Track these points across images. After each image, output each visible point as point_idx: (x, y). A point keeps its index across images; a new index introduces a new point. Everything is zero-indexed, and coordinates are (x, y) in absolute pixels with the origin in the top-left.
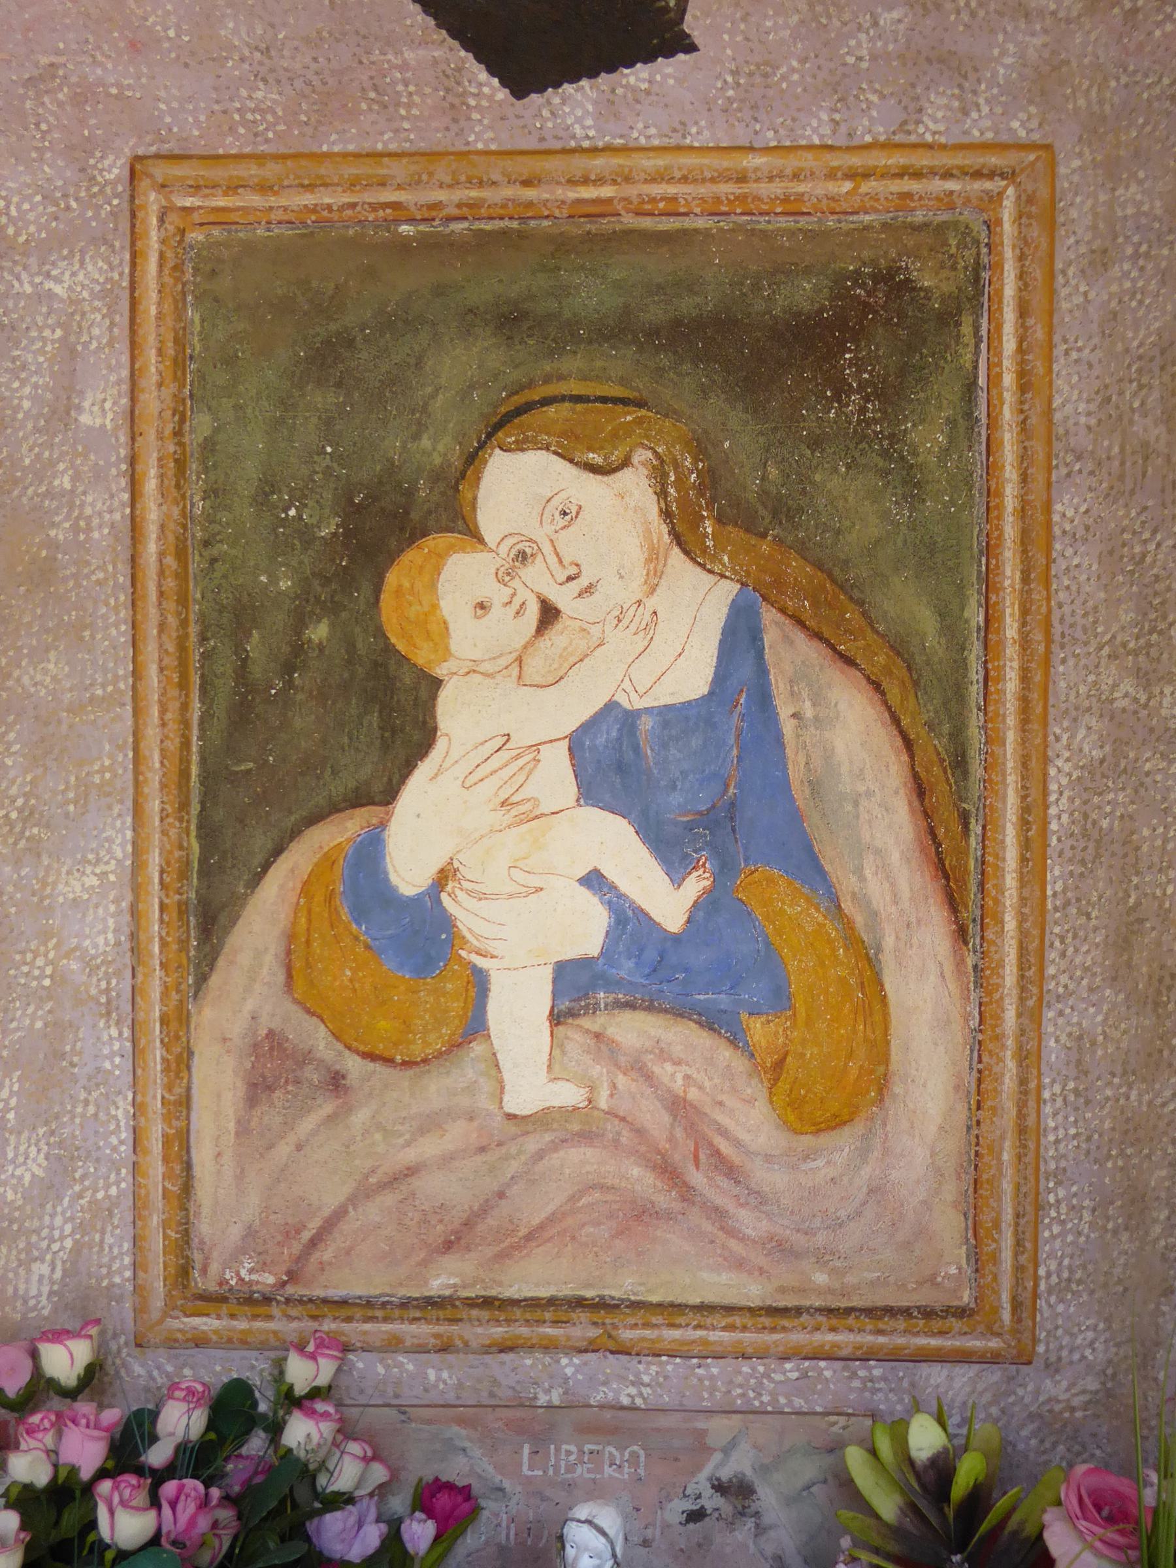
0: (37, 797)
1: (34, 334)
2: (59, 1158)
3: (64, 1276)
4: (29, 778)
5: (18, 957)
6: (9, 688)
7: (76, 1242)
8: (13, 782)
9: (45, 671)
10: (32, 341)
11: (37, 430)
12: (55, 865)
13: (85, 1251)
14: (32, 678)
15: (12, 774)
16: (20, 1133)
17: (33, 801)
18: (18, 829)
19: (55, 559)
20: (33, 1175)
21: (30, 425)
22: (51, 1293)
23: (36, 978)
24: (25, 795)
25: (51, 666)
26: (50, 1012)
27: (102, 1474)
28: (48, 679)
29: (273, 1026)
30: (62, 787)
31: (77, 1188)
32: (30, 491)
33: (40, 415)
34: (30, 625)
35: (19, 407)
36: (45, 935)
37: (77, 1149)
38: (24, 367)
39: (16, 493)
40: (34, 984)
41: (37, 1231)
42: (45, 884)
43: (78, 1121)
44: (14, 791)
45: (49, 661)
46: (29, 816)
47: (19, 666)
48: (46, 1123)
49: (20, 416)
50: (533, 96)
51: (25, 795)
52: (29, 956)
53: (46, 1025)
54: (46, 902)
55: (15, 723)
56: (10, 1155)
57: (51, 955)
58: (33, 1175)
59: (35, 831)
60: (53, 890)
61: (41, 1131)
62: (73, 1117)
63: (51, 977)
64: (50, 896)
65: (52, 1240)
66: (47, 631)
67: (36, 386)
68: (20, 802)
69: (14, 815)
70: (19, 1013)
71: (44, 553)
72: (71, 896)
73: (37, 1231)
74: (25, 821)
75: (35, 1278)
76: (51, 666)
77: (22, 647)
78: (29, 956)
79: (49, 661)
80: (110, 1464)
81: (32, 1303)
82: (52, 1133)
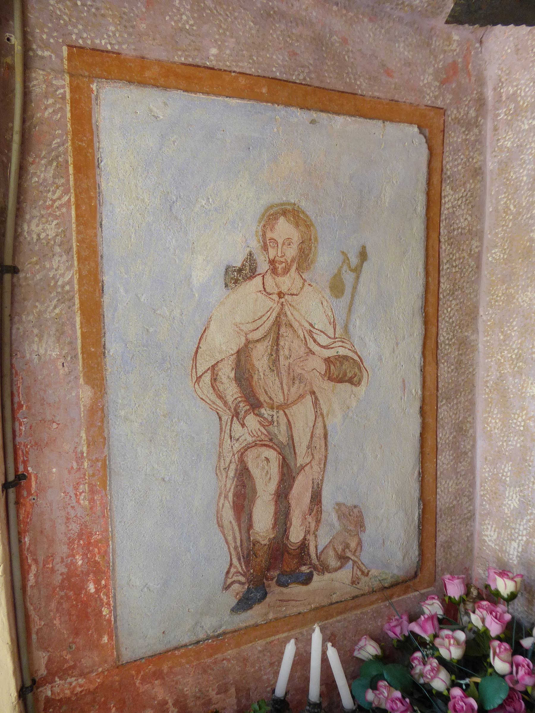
0: (522, 350)
1: (528, 146)
2: (523, 502)
3: (522, 552)
4: (519, 342)
5: (513, 416)
6: (514, 303)
7: (527, 539)
8: (514, 342)
9: (527, 296)
10: (528, 150)
11: (529, 189)
12: (527, 380)
13: (530, 544)
14: (522, 299)
15: (514, 339)
16: (510, 487)
17: (520, 352)
18: (515, 363)
19: (532, 246)
20: (514, 505)
21: (526, 188)
22: (517, 556)
23: (518, 426)
24: (518, 348)
25: (529, 293)
26: (522, 441)
27: (498, 638)
28: (528, 299)
29: (340, 499)
30: (531, 346)
31: (529, 517)
32: (524, 217)
33: (529, 182)
34: (522, 275)
35: (522, 180)
36: (522, 409)
37: (530, 501)
38: (524, 162)
39: (520, 219)
40: (517, 428)
41: (514, 529)
42: (523, 387)
43: (530, 489)
44: (514, 346)
45: (528, 291)
46: (519, 357)
47: (518, 294)
48: (519, 487)
49: (523, 184)
50: (524, 26)
51: (518, 348)
52: (516, 416)
53: (521, 446)
54: (523, 395)
55: (516, 317)
56: (507, 495)
57: (524, 417)
58: (514, 505)
59: (521, 364)
60: (526, 390)
61: (518, 489)
62: (529, 487)
63: (523, 426)
64: (524, 392)
65: (519, 535)
66: (528, 278)
67: (528, 170)
68: (516, 351)
69: (514, 357)
70: (512, 438)
71: (528, 244)
72: (532, 394)
73: (514, 529)
74: (517, 359)
75: (512, 547)
76: (529, 293)
77: (519, 286)
78: (516, 416)
79: (528, 291)
80: (502, 636)
81: (511, 556)
82: (521, 491)
